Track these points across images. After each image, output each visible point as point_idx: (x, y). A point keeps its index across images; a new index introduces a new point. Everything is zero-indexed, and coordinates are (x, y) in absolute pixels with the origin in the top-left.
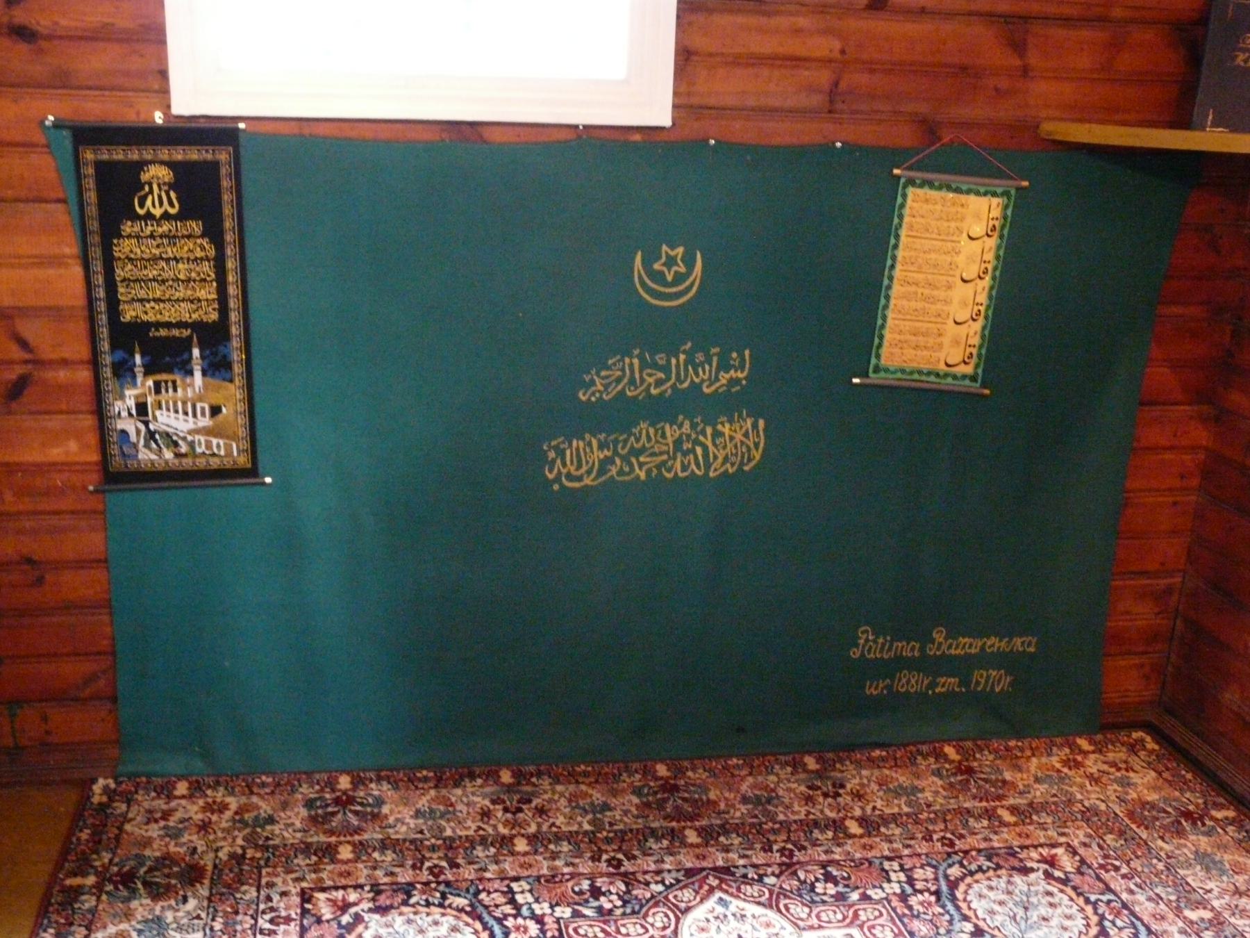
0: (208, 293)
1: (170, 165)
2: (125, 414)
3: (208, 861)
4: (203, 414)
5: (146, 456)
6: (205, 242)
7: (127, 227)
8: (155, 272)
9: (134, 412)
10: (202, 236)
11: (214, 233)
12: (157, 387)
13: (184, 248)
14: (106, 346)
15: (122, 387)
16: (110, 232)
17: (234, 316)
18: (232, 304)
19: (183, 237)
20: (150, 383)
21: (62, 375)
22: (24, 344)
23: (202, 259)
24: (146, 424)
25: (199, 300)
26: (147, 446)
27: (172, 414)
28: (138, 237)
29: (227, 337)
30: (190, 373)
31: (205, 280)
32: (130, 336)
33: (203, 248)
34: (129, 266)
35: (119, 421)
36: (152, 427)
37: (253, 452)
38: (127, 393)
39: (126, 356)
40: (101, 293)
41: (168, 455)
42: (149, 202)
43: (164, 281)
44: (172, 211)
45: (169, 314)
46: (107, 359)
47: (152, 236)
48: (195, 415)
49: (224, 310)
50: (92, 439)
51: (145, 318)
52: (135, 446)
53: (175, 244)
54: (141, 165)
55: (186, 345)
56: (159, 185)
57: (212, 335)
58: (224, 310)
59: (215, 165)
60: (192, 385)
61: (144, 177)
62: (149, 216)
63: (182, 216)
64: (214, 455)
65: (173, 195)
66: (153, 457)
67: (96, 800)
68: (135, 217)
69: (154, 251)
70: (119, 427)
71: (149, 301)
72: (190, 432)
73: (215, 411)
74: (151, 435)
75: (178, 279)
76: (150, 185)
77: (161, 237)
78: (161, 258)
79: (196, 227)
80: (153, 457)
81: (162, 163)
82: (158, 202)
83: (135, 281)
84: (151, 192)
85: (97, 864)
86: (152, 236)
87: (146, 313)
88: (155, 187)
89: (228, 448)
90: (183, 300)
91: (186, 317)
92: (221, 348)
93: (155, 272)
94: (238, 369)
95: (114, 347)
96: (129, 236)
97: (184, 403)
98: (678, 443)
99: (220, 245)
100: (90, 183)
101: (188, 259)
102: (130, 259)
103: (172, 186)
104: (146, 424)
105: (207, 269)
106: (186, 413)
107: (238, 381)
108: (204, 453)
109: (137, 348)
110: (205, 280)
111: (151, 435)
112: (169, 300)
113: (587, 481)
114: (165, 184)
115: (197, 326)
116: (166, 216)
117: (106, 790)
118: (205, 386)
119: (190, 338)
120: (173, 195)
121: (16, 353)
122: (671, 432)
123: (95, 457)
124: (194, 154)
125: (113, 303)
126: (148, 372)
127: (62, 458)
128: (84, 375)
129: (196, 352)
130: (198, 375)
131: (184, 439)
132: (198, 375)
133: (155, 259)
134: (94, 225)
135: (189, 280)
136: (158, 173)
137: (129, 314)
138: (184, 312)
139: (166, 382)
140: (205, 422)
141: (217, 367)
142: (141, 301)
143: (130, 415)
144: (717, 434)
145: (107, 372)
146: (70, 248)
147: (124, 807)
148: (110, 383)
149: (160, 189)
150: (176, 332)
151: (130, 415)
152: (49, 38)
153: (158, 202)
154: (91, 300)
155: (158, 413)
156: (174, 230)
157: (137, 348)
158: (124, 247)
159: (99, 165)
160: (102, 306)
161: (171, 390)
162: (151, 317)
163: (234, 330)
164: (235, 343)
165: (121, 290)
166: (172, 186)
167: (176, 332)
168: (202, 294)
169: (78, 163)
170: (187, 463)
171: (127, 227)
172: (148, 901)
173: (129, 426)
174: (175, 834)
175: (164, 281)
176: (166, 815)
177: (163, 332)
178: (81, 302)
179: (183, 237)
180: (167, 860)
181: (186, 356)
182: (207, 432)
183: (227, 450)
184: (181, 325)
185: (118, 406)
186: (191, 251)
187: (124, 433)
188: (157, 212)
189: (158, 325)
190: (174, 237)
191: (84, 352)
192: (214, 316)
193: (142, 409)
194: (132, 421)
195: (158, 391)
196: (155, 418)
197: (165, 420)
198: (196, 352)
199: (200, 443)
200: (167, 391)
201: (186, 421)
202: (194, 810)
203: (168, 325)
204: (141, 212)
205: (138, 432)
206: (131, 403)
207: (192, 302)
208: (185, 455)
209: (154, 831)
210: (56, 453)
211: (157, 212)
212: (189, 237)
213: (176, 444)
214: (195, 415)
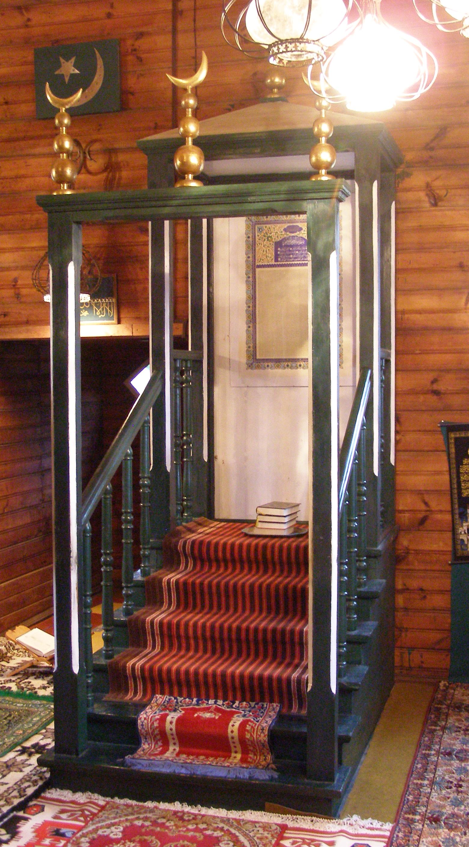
2: (463, 533)
14: (456, 506)
15: (462, 523)
21: (439, 516)
22: (426, 504)
38: (464, 524)
40: (455, 486)
46: (457, 511)
50: (450, 542)
67: (441, 688)
70: (461, 538)
85: (419, 811)
95: (460, 506)
117: (445, 685)
121: (423, 507)
123: (450, 549)
127: (437, 549)
128: (448, 517)
143: (465, 533)
145: (457, 516)
146: (446, 468)
147: (453, 691)
148: (458, 521)
151: (465, 533)
152: (444, 394)
154: (451, 488)
157: (468, 507)
160: (455, 491)
165: (463, 485)
169: (448, 438)
172: (446, 830)
178: (448, 488)
185: (461, 530)
191: (449, 508)
194: (465, 535)
210: (435, 547)
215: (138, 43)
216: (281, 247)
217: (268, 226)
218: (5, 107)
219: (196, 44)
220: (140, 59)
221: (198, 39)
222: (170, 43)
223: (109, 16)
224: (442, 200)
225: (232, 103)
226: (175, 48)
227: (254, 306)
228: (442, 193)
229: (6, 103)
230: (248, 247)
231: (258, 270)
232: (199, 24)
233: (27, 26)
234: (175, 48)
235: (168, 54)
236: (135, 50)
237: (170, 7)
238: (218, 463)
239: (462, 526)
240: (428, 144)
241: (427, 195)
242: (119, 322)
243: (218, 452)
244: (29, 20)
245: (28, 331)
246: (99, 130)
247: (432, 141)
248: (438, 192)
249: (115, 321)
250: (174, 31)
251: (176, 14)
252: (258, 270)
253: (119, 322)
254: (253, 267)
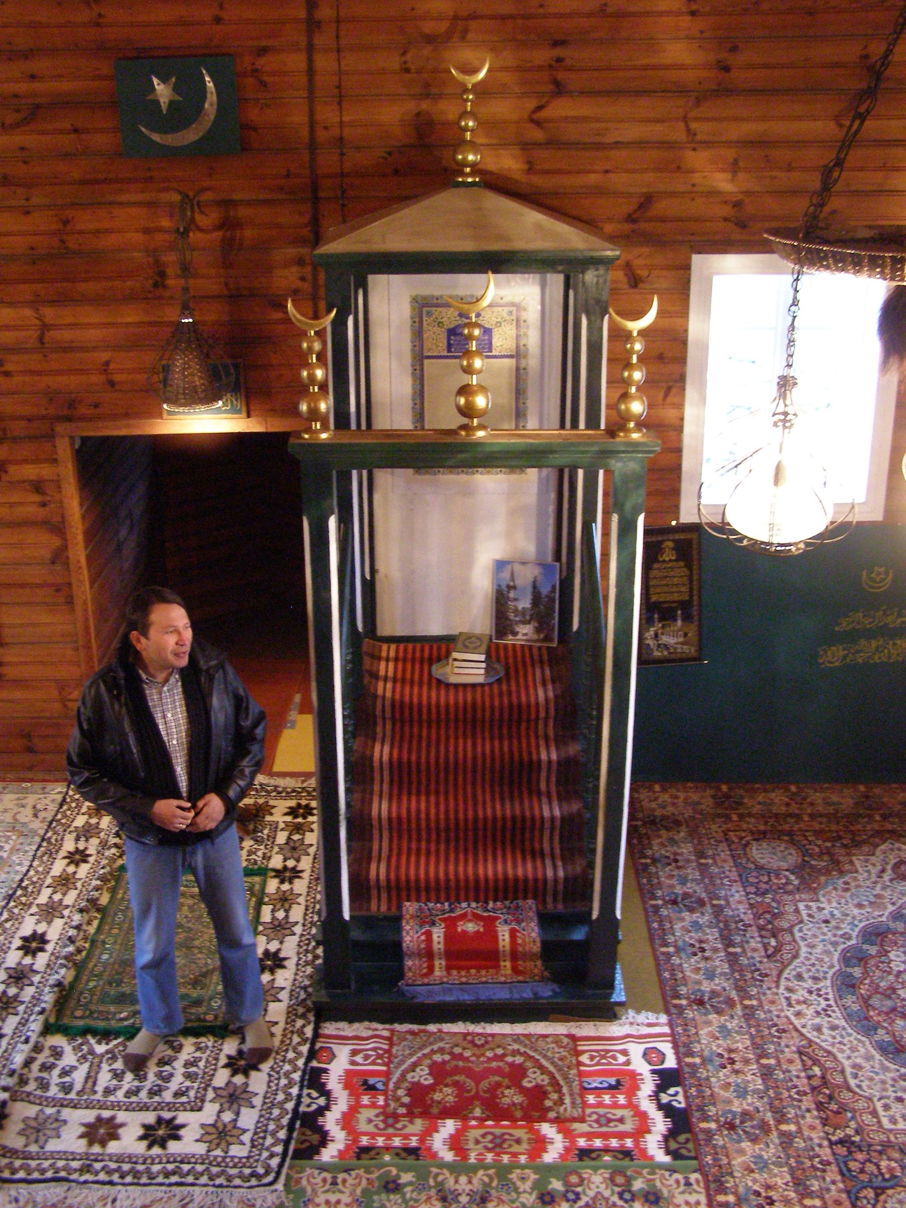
1: (674, 541)
3: (680, 818)
7: (656, 566)
11: (689, 566)
12: (663, 627)
13: (678, 572)
17: (695, 598)
18: (695, 593)
30: (676, 620)
45: (669, 598)
49: (691, 595)
54: (662, 541)
55: (674, 610)
57: (685, 605)
58: (691, 595)
62: (664, 561)
63: (676, 560)
68: (658, 561)
73: (686, 635)
74: (659, 645)
79: (682, 564)
91: (676, 599)
98: (877, 648)
99: (691, 571)
105: (685, 579)
107: (696, 623)
111: (659, 645)
113: (837, 664)
116: (671, 561)
118: (683, 626)
122: (874, 644)
129: (679, 612)
132: (679, 623)
136: (670, 544)
137: (654, 598)
138: (676, 597)
140: (681, 639)
141: (687, 618)
144: (895, 644)
163: (695, 603)
164: (695, 608)
170: (673, 656)
174: (664, 807)
176: (656, 799)
177: (666, 605)
180: (664, 818)
182: (682, 643)
192: (687, 598)
193: (656, 635)
197: (665, 639)
198: (679, 612)
202: (665, 797)
206: (652, 633)
209: (653, 805)
215: (262, 61)
216: (455, 334)
217: (439, 309)
218: (74, 136)
219: (340, 70)
220: (264, 84)
221: (343, 63)
222: (303, 65)
223: (218, 20)
224: (642, 281)
225: (388, 150)
226: (311, 71)
227: (422, 403)
228: (643, 273)
229: (76, 131)
230: (413, 333)
231: (426, 361)
232: (343, 41)
233: (98, 25)
234: (311, 71)
235: (303, 79)
236: (256, 70)
237: (302, 14)
238: (379, 577)
240: (630, 215)
241: (626, 275)
242: (249, 416)
243: (380, 565)
244: (100, 15)
245: (128, 426)
246: (210, 175)
247: (635, 211)
248: (639, 272)
249: (244, 414)
250: (310, 49)
251: (313, 25)
252: (426, 361)
253: (249, 416)
254: (419, 358)
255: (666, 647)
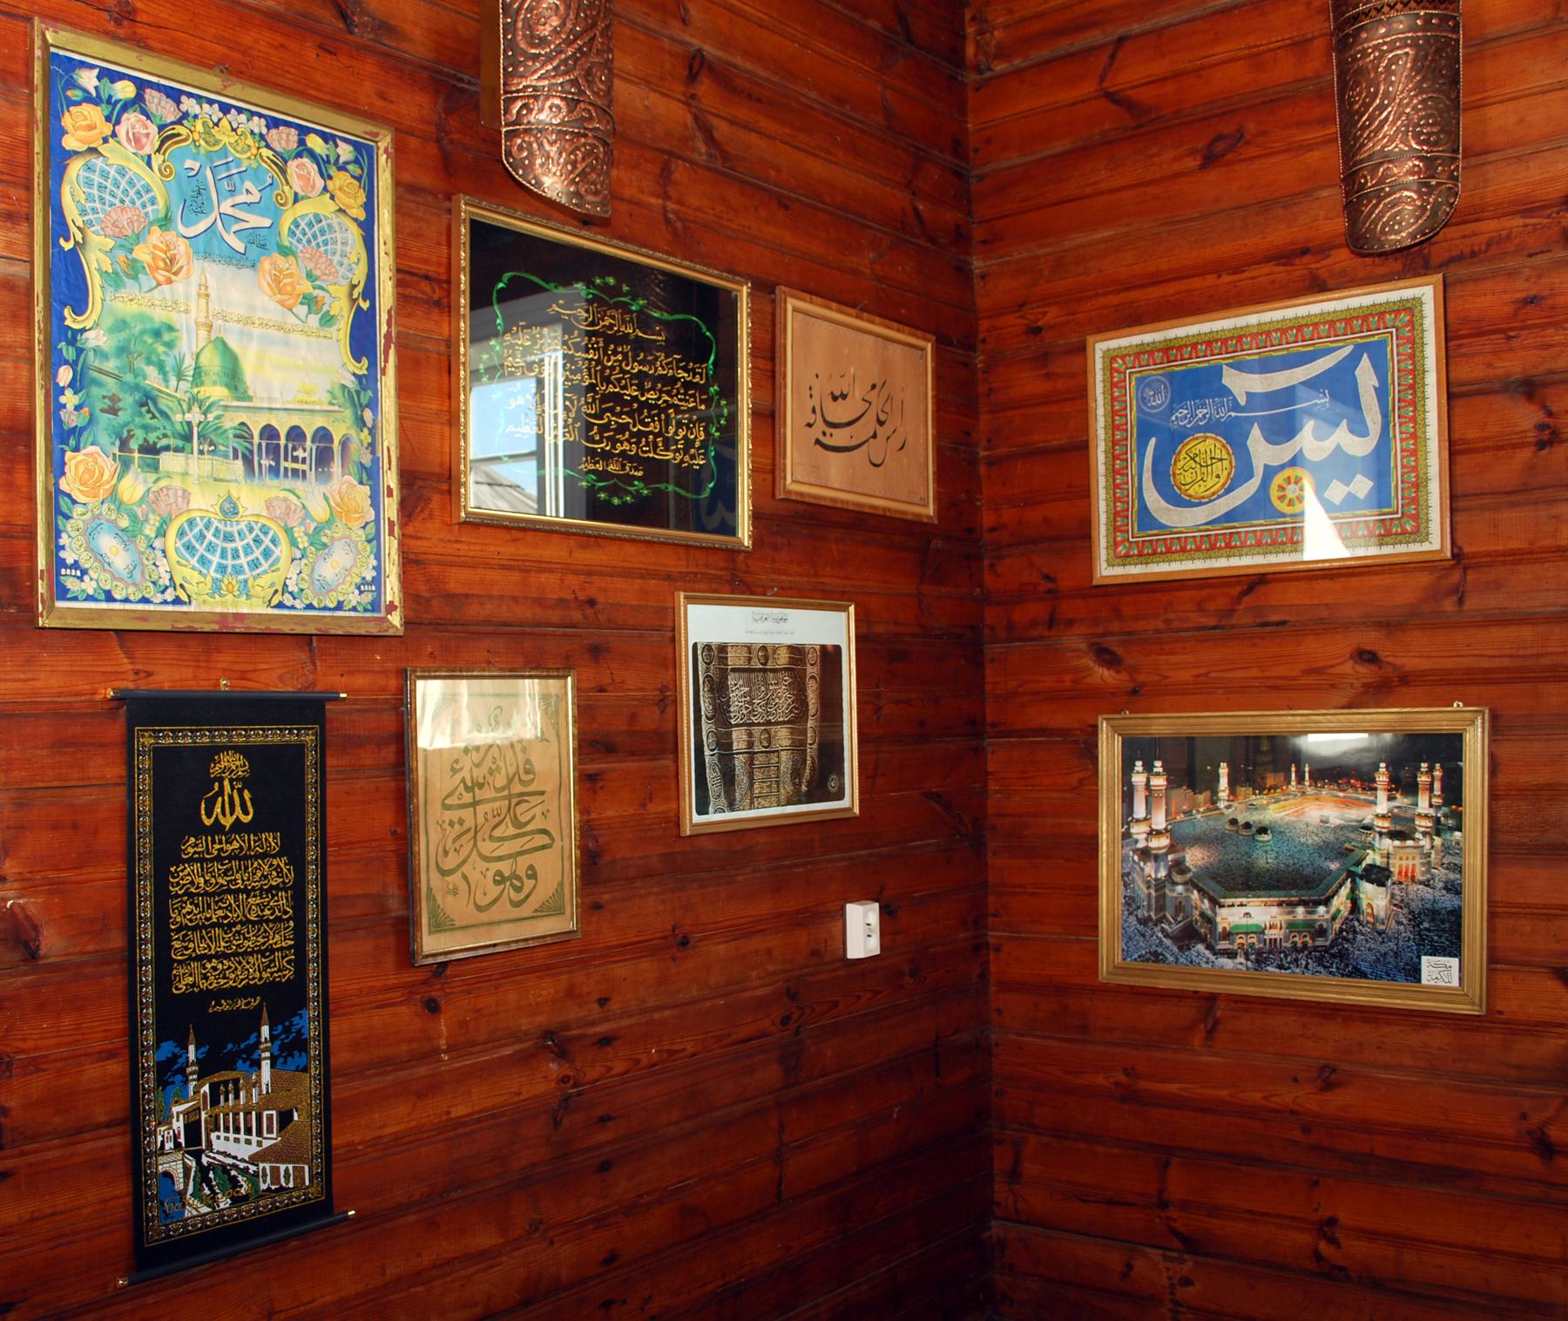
0: (280, 939)
2: (169, 1145)
4: (270, 1131)
5: (196, 1209)
6: (281, 862)
7: (191, 847)
8: (220, 913)
9: (182, 1140)
10: (279, 855)
11: (293, 850)
14: (150, 1036)
16: (167, 856)
17: (312, 971)
19: (257, 856)
20: (206, 1088)
23: (277, 888)
24: (197, 1155)
25: (273, 951)
26: (197, 1194)
27: (232, 1136)
28: (202, 860)
29: (303, 1002)
30: (257, 1064)
31: (279, 919)
32: (183, 1015)
33: (280, 873)
34: (189, 907)
35: (161, 1159)
36: (205, 1160)
37: (326, 1175)
38: (175, 1109)
39: (177, 1050)
41: (224, 1203)
42: (218, 810)
43: (232, 925)
44: (246, 819)
47: (219, 859)
48: (259, 1134)
49: (300, 963)
51: (204, 985)
52: (182, 1194)
53: (246, 868)
54: (212, 752)
55: (251, 1022)
56: (231, 781)
57: (283, 1000)
58: (300, 963)
59: (300, 748)
60: (258, 1083)
61: (215, 770)
62: (217, 827)
63: (255, 828)
64: (282, 1189)
65: (247, 795)
66: (205, 1210)
68: (200, 830)
69: (220, 881)
71: (209, 958)
72: (254, 1159)
73: (285, 1118)
74: (203, 1171)
75: (249, 921)
76: (221, 780)
77: (231, 858)
78: (229, 891)
79: (272, 840)
80: (205, 1210)
81: (237, 749)
82: (230, 808)
83: (194, 929)
84: (221, 792)
86: (219, 859)
87: (205, 977)
88: (226, 783)
89: (299, 1172)
90: (251, 954)
92: (296, 1020)
93: (220, 913)
94: (314, 1049)
96: (191, 860)
97: (247, 1114)
99: (299, 864)
100: (145, 782)
101: (261, 889)
102: (191, 895)
103: (247, 783)
104: (197, 1155)
105: (283, 900)
106: (248, 1131)
108: (269, 1189)
109: (192, 1036)
110: (279, 919)
111: (203, 1171)
112: (236, 954)
114: (238, 779)
115: (268, 990)
116: (238, 826)
119: (259, 1008)
120: (247, 795)
124: (272, 736)
125: (164, 964)
126: (204, 1072)
129: (265, 1031)
130: (266, 1066)
131: (245, 1171)
133: (221, 892)
134: (146, 845)
135: (262, 920)
136: (231, 764)
137: (185, 980)
138: (252, 971)
139: (226, 1083)
142: (200, 958)
148: (151, 1100)
149: (233, 788)
150: (241, 1004)
151: (177, 1146)
153: (230, 808)
155: (213, 1136)
156: (245, 846)
157: (192, 1036)
158: (188, 876)
159: (159, 753)
161: (231, 1096)
162: (214, 984)
166: (247, 783)
167: (241, 1004)
168: (277, 940)
171: (191, 847)
173: (174, 1165)
175: (232, 925)
177: (225, 1006)
179: (257, 856)
181: (252, 1039)
183: (293, 1177)
184: (249, 991)
186: (266, 877)
187: (168, 1175)
188: (227, 822)
189: (221, 994)
190: (246, 858)
192: (289, 974)
193: (192, 1129)
195: (215, 1102)
196: (209, 1143)
197: (231, 1147)
198: (265, 1031)
199: (265, 1175)
200: (227, 1100)
201: (248, 1142)
203: (232, 993)
204: (208, 822)
205: (187, 1169)
206: (179, 1125)
207: (262, 953)
208: (245, 1198)
211: (227, 822)
212: (263, 856)
213: (234, 1182)
214: (259, 1134)
239: (166, 1120)
255: (226, 1174)
